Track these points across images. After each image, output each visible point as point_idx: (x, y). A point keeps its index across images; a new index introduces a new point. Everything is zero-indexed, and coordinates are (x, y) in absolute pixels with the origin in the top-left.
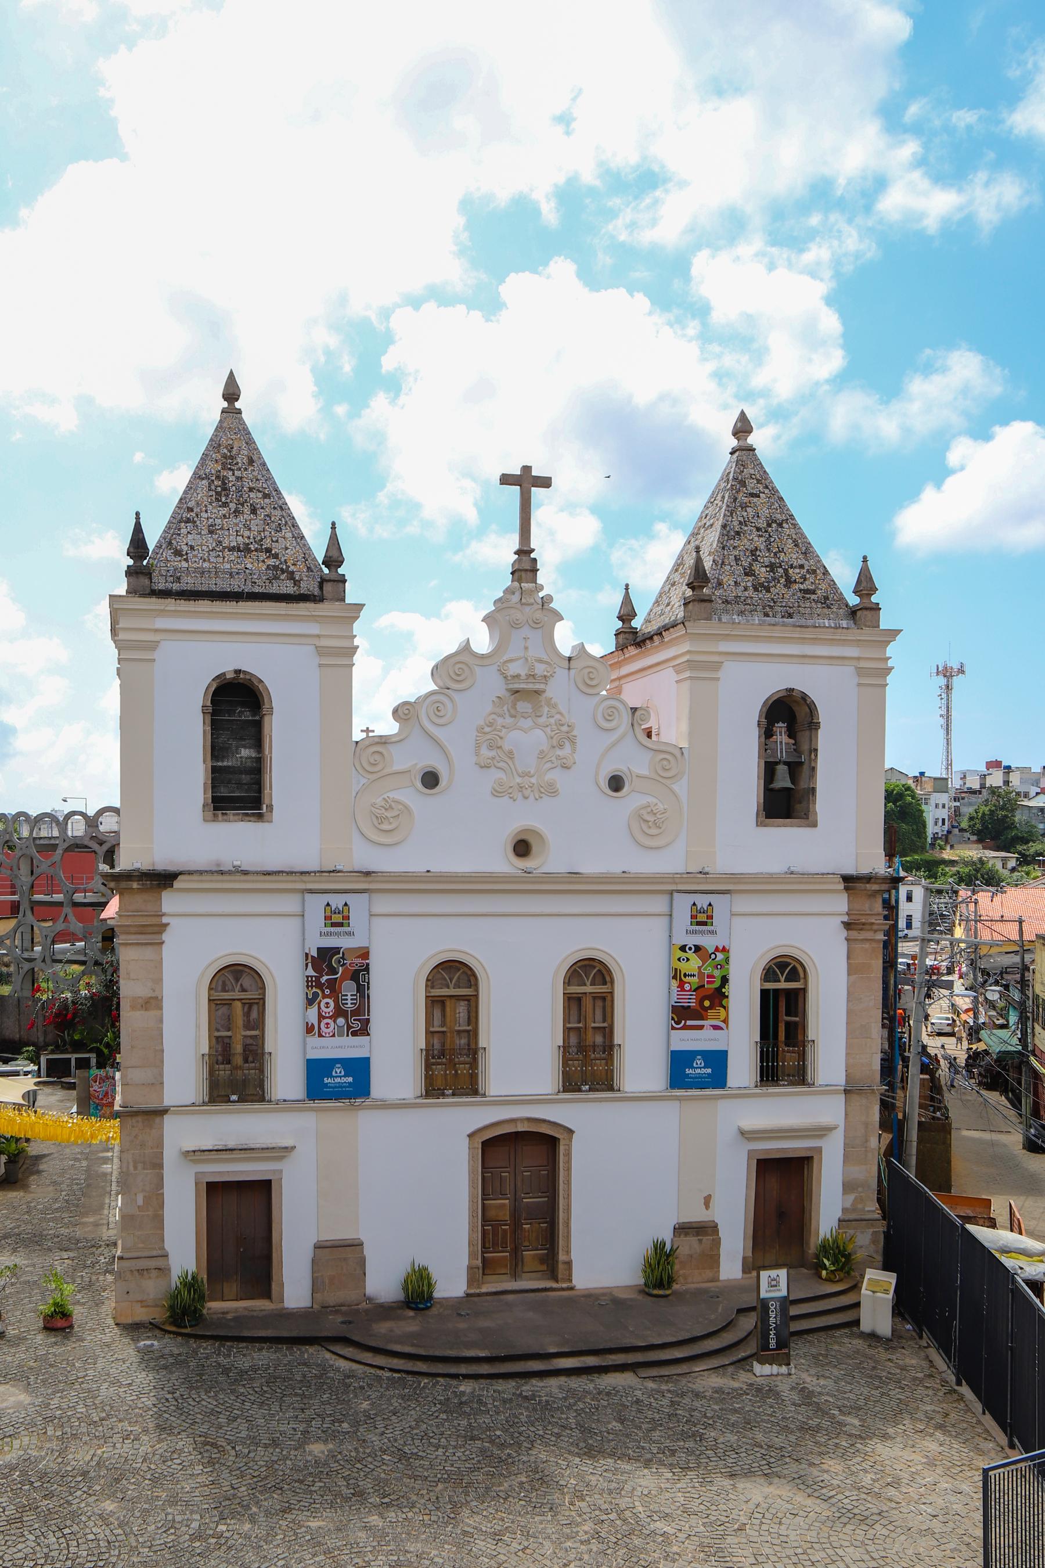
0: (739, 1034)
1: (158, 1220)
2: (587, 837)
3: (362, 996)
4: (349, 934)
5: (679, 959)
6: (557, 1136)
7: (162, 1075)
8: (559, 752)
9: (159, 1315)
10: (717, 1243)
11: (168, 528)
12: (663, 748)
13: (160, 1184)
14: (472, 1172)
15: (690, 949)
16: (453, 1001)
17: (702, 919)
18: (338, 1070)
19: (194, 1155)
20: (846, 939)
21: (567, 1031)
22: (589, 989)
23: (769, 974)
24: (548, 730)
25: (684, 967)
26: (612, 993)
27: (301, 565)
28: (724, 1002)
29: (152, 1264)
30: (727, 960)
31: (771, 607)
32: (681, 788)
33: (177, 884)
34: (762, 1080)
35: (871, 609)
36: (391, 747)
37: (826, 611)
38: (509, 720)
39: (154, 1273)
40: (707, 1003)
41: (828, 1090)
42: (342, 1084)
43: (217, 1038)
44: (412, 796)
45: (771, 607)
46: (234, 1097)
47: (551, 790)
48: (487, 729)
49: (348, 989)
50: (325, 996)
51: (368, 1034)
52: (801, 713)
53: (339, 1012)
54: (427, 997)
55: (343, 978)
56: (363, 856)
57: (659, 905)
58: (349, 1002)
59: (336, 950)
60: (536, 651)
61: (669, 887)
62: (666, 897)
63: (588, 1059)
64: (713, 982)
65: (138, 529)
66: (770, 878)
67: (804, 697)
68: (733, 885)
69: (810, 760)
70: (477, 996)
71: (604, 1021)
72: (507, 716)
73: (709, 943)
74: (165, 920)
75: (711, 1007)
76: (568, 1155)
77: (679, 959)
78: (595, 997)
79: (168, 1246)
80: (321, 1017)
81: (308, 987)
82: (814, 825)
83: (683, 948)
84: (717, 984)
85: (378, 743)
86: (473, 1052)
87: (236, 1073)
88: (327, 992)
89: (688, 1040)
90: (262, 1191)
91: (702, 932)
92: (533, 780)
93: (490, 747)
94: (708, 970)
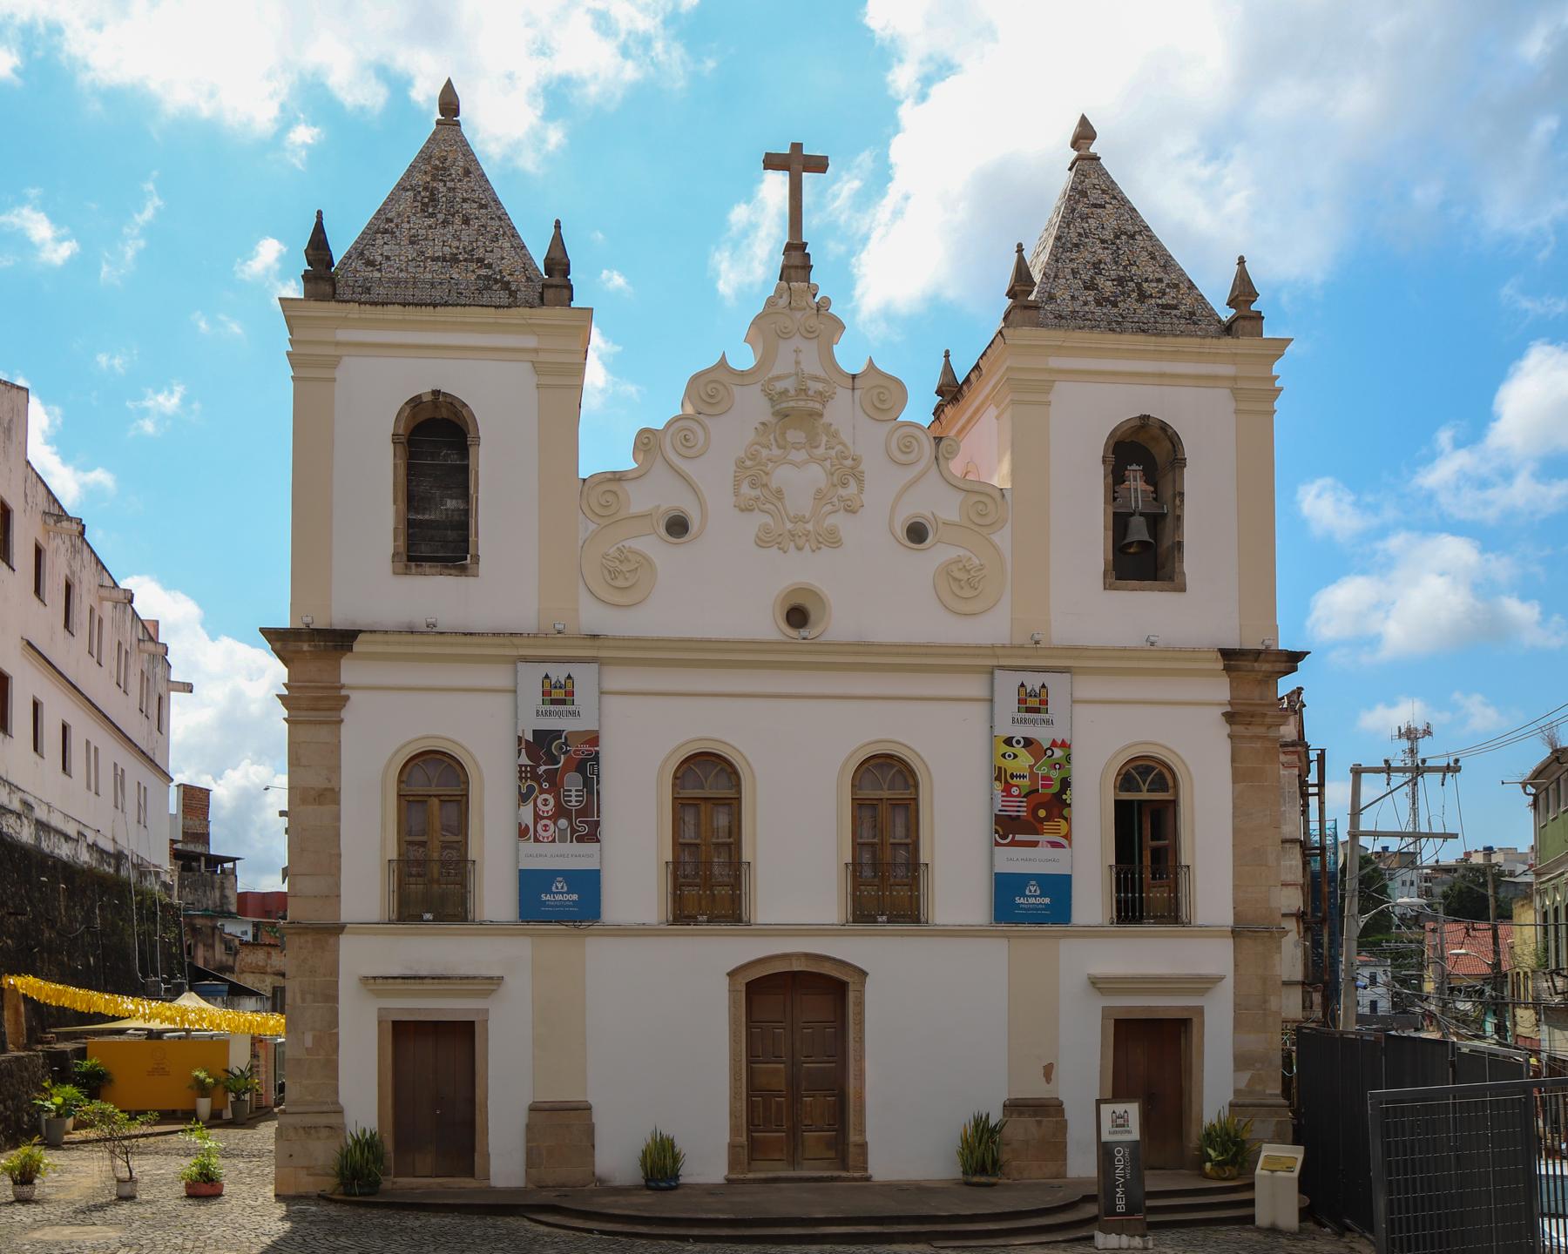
0: (1087, 853)
1: (331, 1067)
2: (878, 594)
3: (590, 793)
4: (573, 714)
6: (845, 978)
7: (338, 885)
8: (841, 492)
9: (329, 1184)
10: (1062, 1127)
11: (361, 238)
12: (976, 488)
13: (334, 1022)
14: (734, 1021)
15: (1018, 742)
17: (1033, 704)
18: (560, 885)
19: (375, 983)
20: (1230, 736)
21: (857, 846)
22: (886, 794)
23: (1126, 780)
25: (1010, 765)
26: (916, 800)
27: (519, 276)
28: (1065, 812)
29: (323, 1120)
30: (1068, 758)
31: (1118, 323)
32: (1003, 538)
33: (358, 647)
34: (1119, 916)
35: (1251, 318)
36: (627, 486)
37: (1191, 327)
38: (776, 451)
39: (324, 1133)
40: (1042, 813)
41: (1209, 932)
42: (562, 904)
43: (410, 843)
44: (655, 546)
45: (1118, 323)
46: (428, 916)
47: (832, 540)
48: (748, 463)
49: (573, 784)
50: (542, 791)
51: (598, 841)
52: (1160, 452)
53: (561, 811)
54: (674, 799)
55: (565, 769)
56: (592, 616)
57: (975, 686)
58: (574, 799)
59: (557, 734)
60: (811, 366)
61: (987, 663)
62: (985, 678)
63: (886, 880)
64: (1049, 786)
65: (319, 230)
66: (1123, 652)
67: (1164, 427)
68: (1074, 662)
69: (1174, 507)
70: (739, 799)
71: (907, 836)
72: (774, 447)
73: (1043, 735)
74: (343, 692)
75: (1048, 818)
76: (860, 1003)
78: (895, 804)
79: (342, 1100)
80: (537, 817)
81: (521, 778)
82: (1182, 589)
83: (1008, 742)
84: (1056, 788)
85: (610, 480)
86: (736, 869)
87: (431, 886)
88: (546, 785)
89: (1017, 860)
90: (460, 1037)
91: (1034, 722)
92: (810, 527)
93: (753, 485)
94: (1043, 771)
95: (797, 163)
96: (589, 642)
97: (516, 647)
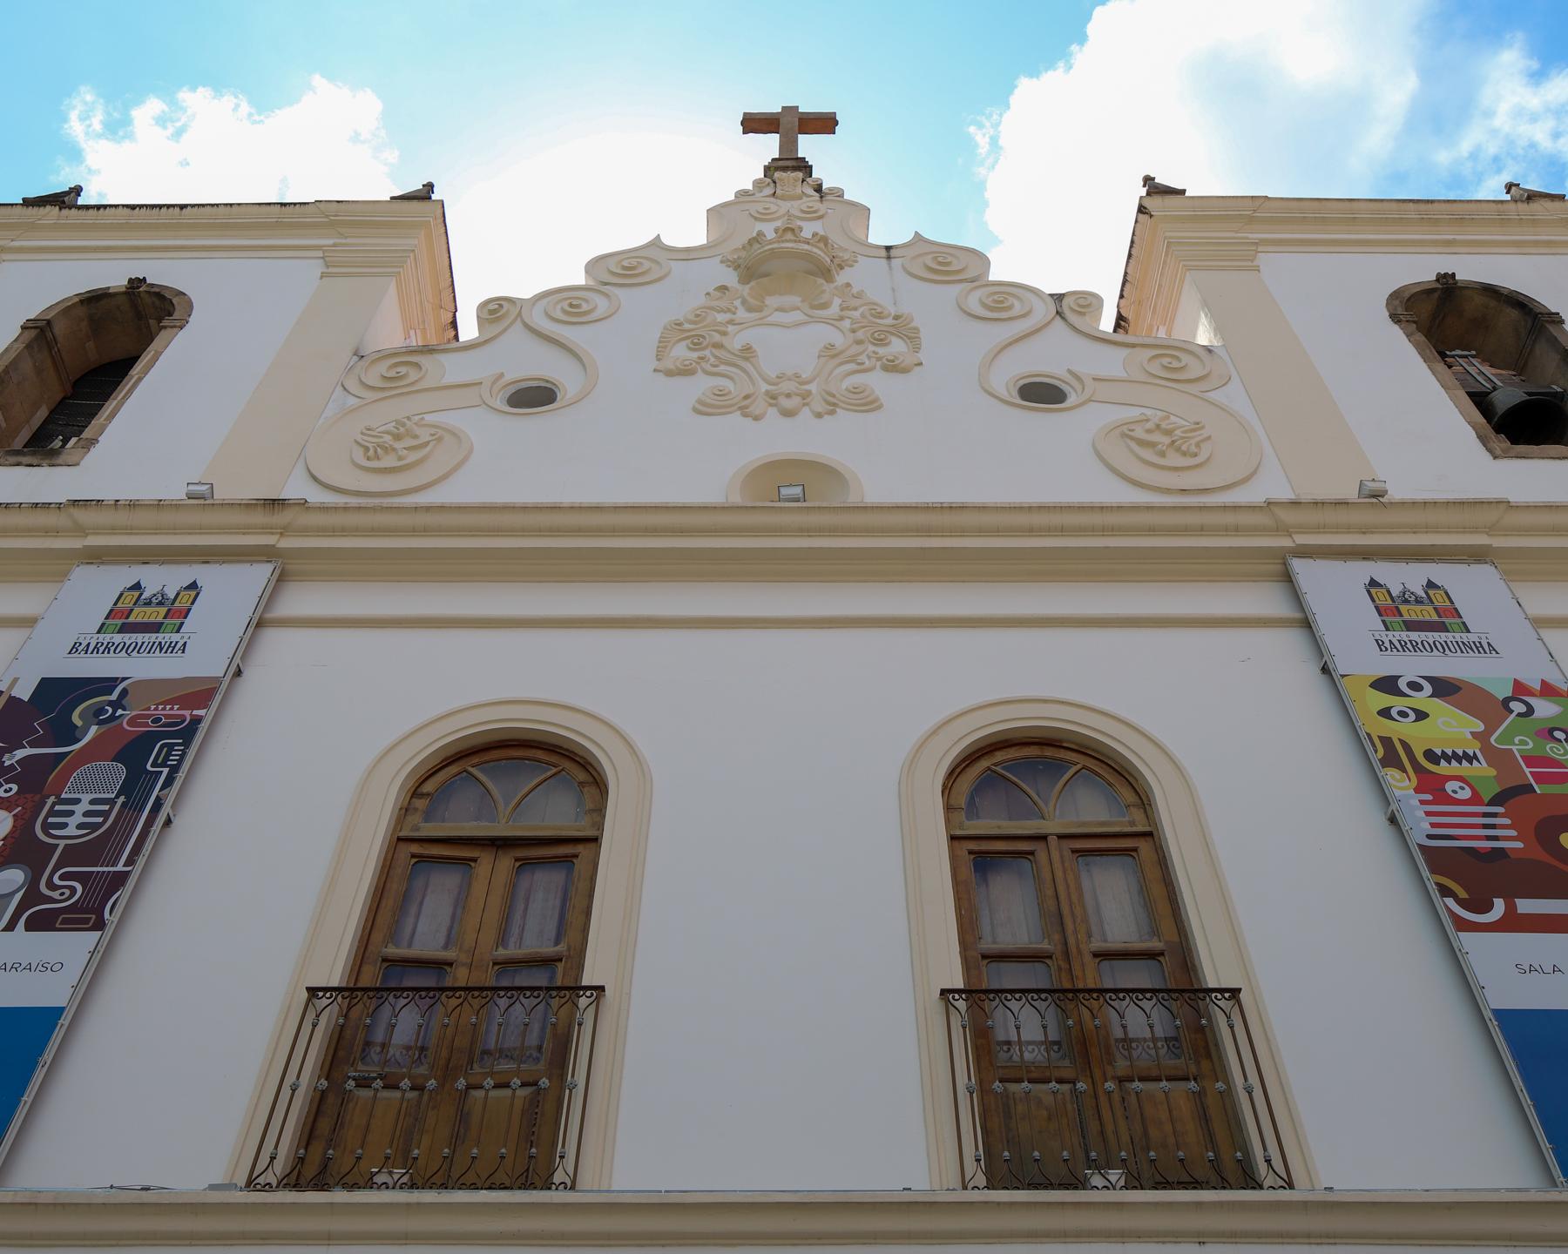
5: (1385, 713)
22: (1051, 826)
24: (847, 324)
25: (1418, 735)
38: (742, 314)
59: (107, 684)
77: (1385, 713)
83: (1387, 684)
95: (789, 125)
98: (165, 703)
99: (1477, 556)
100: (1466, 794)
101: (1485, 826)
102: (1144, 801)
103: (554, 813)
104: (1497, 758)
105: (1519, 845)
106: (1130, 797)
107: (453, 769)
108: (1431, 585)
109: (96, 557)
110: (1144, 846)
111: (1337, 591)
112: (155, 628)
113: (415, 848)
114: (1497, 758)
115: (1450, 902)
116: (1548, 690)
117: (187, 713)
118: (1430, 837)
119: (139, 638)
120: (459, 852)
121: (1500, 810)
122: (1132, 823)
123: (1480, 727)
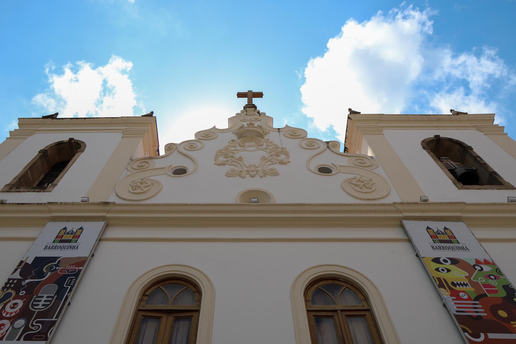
3: (59, 299)
5: (437, 270)
15: (445, 261)
16: (171, 318)
22: (338, 307)
50: (17, 297)
54: (138, 310)
70: (198, 311)
77: (437, 270)
83: (436, 260)
96: (101, 208)
97: (50, 211)
98: (71, 265)
99: (458, 219)
100: (466, 297)
101: (474, 308)
102: (366, 299)
103: (186, 303)
104: (474, 285)
105: (486, 314)
106: (362, 297)
107: (155, 287)
108: (445, 228)
109: (54, 219)
110: (367, 313)
111: (417, 230)
112: (69, 241)
113: (143, 313)
114: (474, 285)
115: (466, 334)
116: (486, 262)
117: (77, 268)
118: (457, 311)
119: (65, 244)
120: (156, 315)
121: (478, 302)
122: (363, 306)
123: (467, 274)
